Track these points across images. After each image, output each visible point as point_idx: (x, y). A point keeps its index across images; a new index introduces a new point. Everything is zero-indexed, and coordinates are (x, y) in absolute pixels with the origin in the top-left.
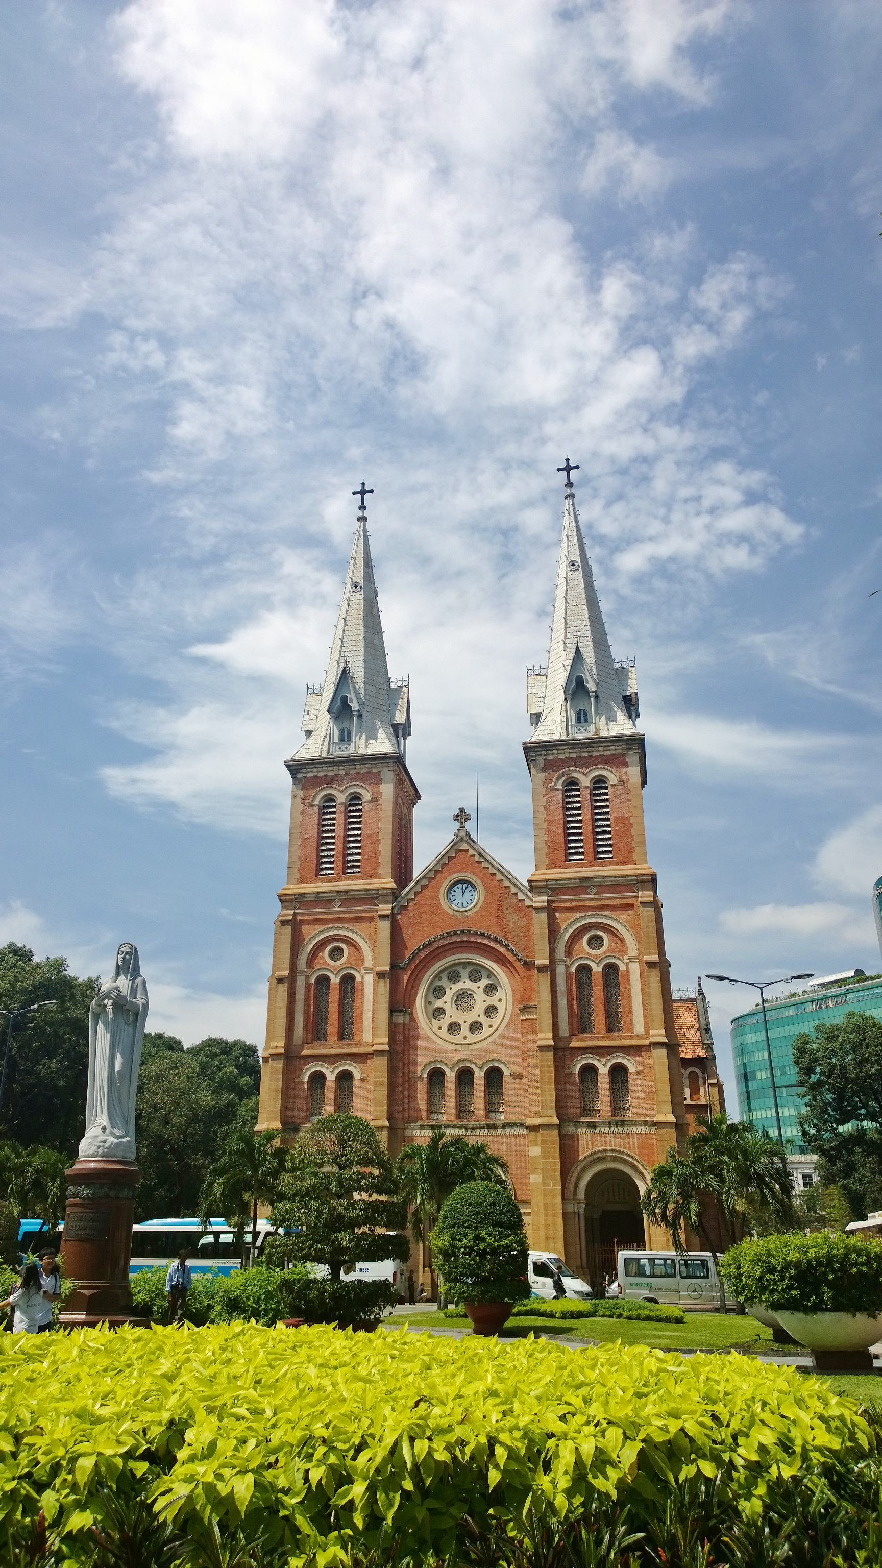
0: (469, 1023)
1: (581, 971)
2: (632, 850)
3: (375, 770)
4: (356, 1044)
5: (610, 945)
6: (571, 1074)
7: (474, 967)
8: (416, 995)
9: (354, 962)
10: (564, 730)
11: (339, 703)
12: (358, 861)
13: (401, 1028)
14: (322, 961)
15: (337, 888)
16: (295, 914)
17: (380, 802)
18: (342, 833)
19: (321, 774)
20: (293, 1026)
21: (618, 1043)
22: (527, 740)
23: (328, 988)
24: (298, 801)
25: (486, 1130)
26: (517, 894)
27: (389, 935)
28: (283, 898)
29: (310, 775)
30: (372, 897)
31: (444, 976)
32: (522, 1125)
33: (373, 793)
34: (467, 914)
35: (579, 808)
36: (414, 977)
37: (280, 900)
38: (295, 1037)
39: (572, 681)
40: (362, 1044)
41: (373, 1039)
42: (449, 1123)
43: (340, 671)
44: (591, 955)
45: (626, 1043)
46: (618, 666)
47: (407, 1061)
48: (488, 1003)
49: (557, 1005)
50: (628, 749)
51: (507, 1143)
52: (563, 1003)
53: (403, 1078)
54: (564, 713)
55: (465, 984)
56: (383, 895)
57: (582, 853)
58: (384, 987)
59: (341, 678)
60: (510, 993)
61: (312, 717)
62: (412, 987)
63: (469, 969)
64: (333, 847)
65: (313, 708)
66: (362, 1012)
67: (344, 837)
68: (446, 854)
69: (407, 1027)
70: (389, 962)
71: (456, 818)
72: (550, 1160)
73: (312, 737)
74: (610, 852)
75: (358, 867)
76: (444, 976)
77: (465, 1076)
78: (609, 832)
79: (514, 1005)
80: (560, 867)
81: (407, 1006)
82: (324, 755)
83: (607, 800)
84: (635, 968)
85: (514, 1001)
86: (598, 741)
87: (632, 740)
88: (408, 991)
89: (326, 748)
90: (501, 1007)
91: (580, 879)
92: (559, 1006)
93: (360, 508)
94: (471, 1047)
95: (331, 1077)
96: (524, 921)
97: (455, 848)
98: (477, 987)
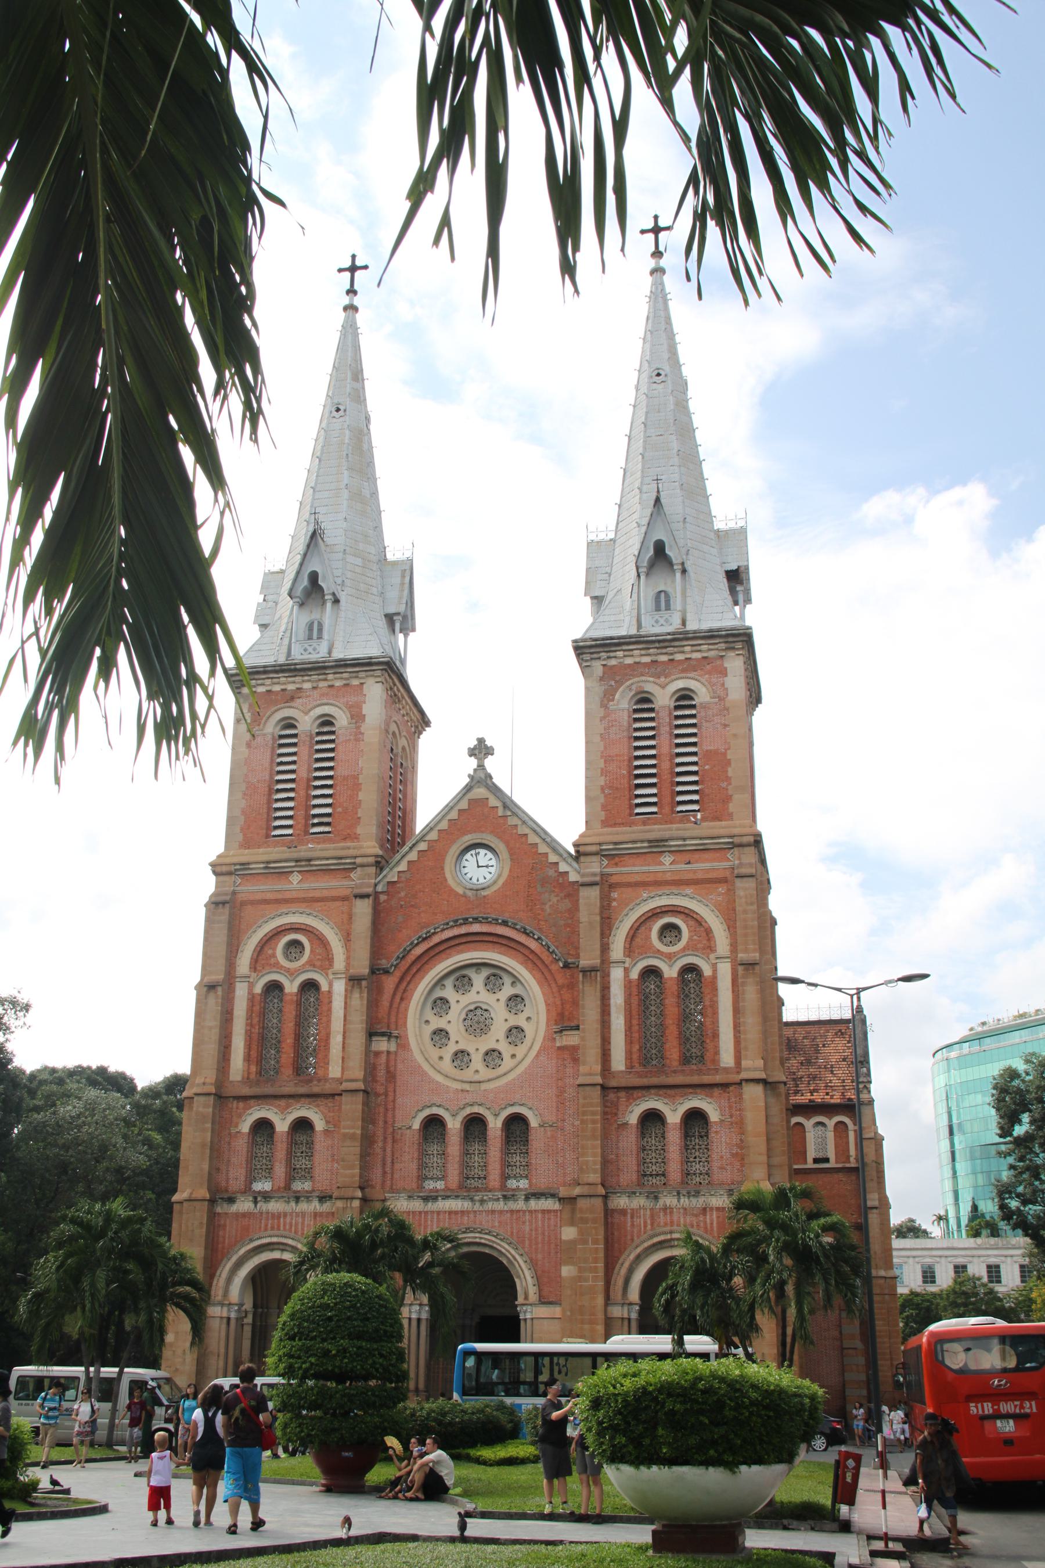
0: (483, 1049)
1: (649, 977)
2: (728, 799)
3: (355, 682)
5: (690, 939)
6: (626, 1124)
8: (407, 1010)
9: (318, 963)
10: (635, 622)
11: (305, 582)
12: (328, 815)
13: (384, 1057)
14: (272, 961)
15: (295, 855)
16: (234, 893)
17: (362, 730)
18: (305, 775)
19: (277, 688)
20: (230, 1054)
21: (695, 1079)
22: (578, 635)
23: (281, 1001)
25: (502, 1203)
26: (557, 863)
28: (218, 869)
29: (261, 689)
31: (449, 982)
32: (553, 1196)
34: (484, 893)
35: (653, 737)
36: (404, 984)
37: (215, 873)
38: (231, 1071)
39: (648, 548)
41: (343, 1073)
42: (449, 1194)
43: (310, 534)
44: (662, 953)
45: (707, 1079)
46: (719, 525)
47: (390, 1106)
48: (514, 1021)
49: (609, 1027)
50: (727, 649)
51: (530, 1222)
52: (618, 1022)
53: (385, 1129)
54: (635, 596)
55: (478, 993)
56: (362, 866)
58: (359, 1001)
59: (308, 546)
62: (402, 999)
63: (485, 972)
64: (292, 795)
67: (309, 780)
69: (392, 1057)
70: (367, 963)
71: (472, 752)
72: (590, 1245)
73: (269, 632)
75: (328, 824)
77: (475, 1125)
78: (695, 773)
79: (547, 1023)
80: (623, 824)
81: (393, 1026)
82: (282, 660)
83: (694, 725)
84: (725, 970)
88: (395, 1005)
89: (285, 649)
91: (650, 841)
92: (613, 1027)
94: (484, 1086)
95: (282, 1126)
96: (567, 904)
97: (470, 796)
98: (496, 1003)
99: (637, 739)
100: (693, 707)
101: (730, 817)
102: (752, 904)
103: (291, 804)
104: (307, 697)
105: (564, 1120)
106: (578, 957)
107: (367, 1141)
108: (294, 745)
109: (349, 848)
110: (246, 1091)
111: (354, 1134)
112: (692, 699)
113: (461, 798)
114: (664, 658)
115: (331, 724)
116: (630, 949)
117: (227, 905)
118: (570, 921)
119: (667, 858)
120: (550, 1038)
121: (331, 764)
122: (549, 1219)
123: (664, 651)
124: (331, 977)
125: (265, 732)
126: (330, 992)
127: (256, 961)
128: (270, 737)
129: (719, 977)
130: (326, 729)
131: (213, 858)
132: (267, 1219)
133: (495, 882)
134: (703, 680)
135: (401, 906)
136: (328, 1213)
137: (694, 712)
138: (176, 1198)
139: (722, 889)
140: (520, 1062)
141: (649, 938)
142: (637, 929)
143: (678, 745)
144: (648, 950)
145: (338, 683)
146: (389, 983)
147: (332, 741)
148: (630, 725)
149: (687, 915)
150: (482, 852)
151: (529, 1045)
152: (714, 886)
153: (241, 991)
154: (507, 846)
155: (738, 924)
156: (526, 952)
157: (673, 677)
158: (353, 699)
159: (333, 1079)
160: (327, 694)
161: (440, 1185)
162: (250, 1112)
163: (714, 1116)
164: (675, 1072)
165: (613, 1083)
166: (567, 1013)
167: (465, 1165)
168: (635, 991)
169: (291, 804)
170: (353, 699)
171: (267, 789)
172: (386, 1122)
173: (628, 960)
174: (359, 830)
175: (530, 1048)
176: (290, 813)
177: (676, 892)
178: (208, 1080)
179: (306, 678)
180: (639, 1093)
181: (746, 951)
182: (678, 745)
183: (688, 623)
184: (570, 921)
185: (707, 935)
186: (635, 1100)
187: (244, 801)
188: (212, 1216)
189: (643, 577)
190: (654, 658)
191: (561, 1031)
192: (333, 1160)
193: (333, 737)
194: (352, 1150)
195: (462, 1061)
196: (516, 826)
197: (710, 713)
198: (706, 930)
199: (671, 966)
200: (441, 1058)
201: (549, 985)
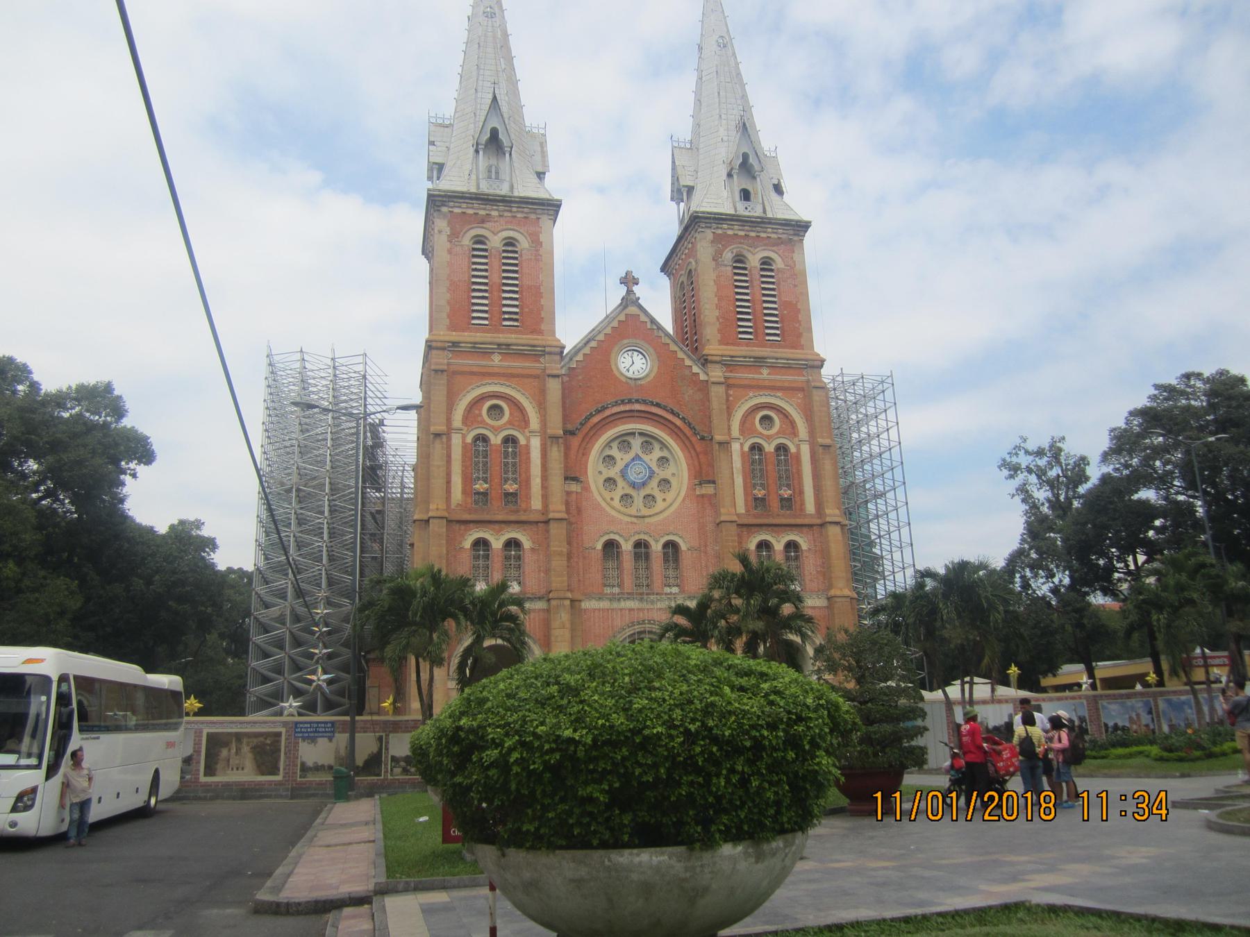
2: (799, 335)
3: (533, 216)
5: (781, 427)
7: (647, 439)
10: (731, 205)
14: (479, 419)
15: (497, 340)
16: (448, 364)
17: (541, 253)
19: (470, 211)
21: (792, 521)
27: (560, 397)
28: (434, 344)
29: (457, 210)
30: (536, 353)
31: (615, 445)
34: (642, 382)
36: (583, 445)
45: (799, 521)
50: (794, 235)
56: (550, 353)
58: (556, 453)
60: (684, 466)
61: (439, 149)
62: (583, 455)
64: (486, 295)
70: (560, 425)
75: (516, 320)
76: (615, 445)
82: (473, 190)
83: (773, 283)
84: (805, 450)
85: (689, 476)
86: (763, 222)
87: (800, 226)
89: (473, 183)
90: (674, 482)
91: (754, 358)
94: (647, 520)
95: (497, 543)
99: (737, 287)
100: (772, 270)
101: (802, 347)
104: (495, 222)
105: (706, 546)
107: (569, 556)
108: (485, 257)
111: (562, 551)
112: (770, 265)
113: (620, 312)
114: (753, 234)
116: (742, 431)
117: (445, 373)
118: (702, 408)
120: (692, 488)
123: (754, 229)
124: (528, 435)
126: (527, 447)
129: (802, 453)
130: (510, 249)
133: (647, 375)
134: (780, 252)
136: (540, 610)
137: (773, 274)
140: (671, 505)
141: (754, 424)
143: (764, 295)
145: (519, 215)
146: (575, 442)
147: (516, 258)
149: (778, 410)
150: (636, 353)
153: (456, 440)
154: (655, 350)
156: (673, 428)
160: (511, 222)
161: (616, 590)
163: (804, 546)
164: (778, 515)
166: (704, 472)
167: (637, 578)
172: (578, 544)
173: (741, 437)
174: (543, 327)
175: (678, 495)
176: (486, 308)
178: (440, 507)
179: (495, 207)
180: (756, 529)
182: (764, 295)
184: (702, 408)
186: (754, 533)
187: (449, 295)
189: (735, 177)
190: (747, 233)
191: (701, 484)
192: (540, 571)
193: (516, 255)
194: (558, 563)
195: (626, 502)
198: (791, 422)
199: (769, 444)
200: (612, 499)
201: (690, 452)
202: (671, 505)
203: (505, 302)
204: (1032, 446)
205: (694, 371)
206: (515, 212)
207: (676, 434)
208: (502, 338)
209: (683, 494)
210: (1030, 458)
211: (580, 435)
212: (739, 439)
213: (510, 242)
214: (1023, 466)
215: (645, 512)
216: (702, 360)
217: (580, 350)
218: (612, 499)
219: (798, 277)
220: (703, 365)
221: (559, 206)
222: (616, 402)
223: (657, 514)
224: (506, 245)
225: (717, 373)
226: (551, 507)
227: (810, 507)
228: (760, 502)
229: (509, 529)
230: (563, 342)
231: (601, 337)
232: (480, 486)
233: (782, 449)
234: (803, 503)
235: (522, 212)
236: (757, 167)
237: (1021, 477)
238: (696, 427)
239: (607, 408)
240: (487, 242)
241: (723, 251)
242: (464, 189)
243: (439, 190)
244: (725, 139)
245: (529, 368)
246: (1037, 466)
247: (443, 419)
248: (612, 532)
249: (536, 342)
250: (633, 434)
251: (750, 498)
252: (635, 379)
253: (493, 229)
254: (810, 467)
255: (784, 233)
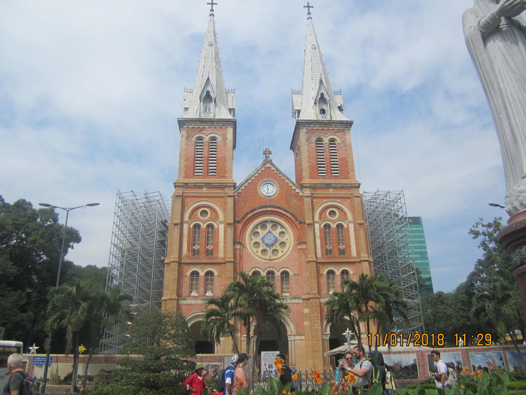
2: (348, 173)
3: (224, 127)
4: (215, 258)
5: (339, 216)
8: (245, 235)
9: (214, 218)
13: (239, 250)
15: (205, 182)
16: (183, 193)
17: (227, 142)
21: (345, 260)
24: (184, 138)
28: (177, 184)
30: (223, 186)
31: (259, 227)
33: (223, 138)
34: (272, 197)
35: (323, 152)
37: (175, 186)
39: (319, 95)
40: (218, 258)
44: (331, 220)
45: (348, 260)
52: (318, 241)
56: (229, 186)
57: (325, 173)
58: (230, 231)
64: (202, 162)
65: (188, 98)
66: (218, 243)
67: (208, 158)
68: (261, 169)
69: (241, 250)
74: (338, 173)
75: (215, 172)
76: (259, 227)
78: (337, 164)
79: (294, 241)
80: (315, 178)
82: (198, 117)
83: (336, 150)
84: (351, 226)
86: (330, 123)
89: (198, 114)
91: (326, 184)
93: (211, 11)
94: (273, 261)
95: (202, 273)
96: (299, 203)
97: (266, 166)
99: (318, 152)
100: (335, 144)
101: (350, 178)
102: (360, 205)
103: (202, 165)
106: (304, 219)
108: (202, 146)
109: (224, 180)
110: (189, 261)
111: (231, 276)
113: (262, 167)
115: (216, 140)
116: (320, 218)
118: (300, 208)
119: (331, 190)
121: (216, 153)
122: (299, 306)
125: (192, 140)
126: (218, 228)
127: (191, 217)
128: (194, 142)
129: (350, 228)
130: (213, 141)
131: (175, 181)
132: (198, 306)
133: (275, 194)
135: (243, 200)
137: (336, 146)
138: (163, 298)
139: (349, 200)
140: (285, 254)
141: (326, 215)
142: (322, 212)
143: (331, 155)
144: (326, 219)
145: (217, 127)
146: (240, 226)
147: (216, 146)
148: (316, 148)
149: (338, 208)
151: (288, 248)
152: (346, 199)
153: (186, 226)
155: (356, 211)
157: (329, 134)
158: (223, 132)
159: (220, 257)
160: (214, 130)
162: (190, 268)
164: (338, 258)
165: (318, 261)
168: (322, 232)
169: (202, 165)
170: (223, 132)
171: (193, 159)
173: (320, 221)
174: (227, 175)
176: (202, 168)
177: (335, 200)
178: (175, 257)
179: (207, 124)
181: (359, 220)
182: (331, 155)
183: (332, 118)
185: (345, 214)
186: (325, 267)
187: (185, 163)
188: (178, 305)
189: (317, 104)
193: (216, 144)
196: (281, 177)
197: (341, 146)
200: (257, 252)
202: (285, 254)
203: (210, 165)
204: (485, 223)
205: (297, 192)
206: (216, 126)
207: (288, 221)
208: (208, 180)
209: (291, 248)
210: (485, 228)
211: (242, 223)
212: (319, 222)
213: (213, 139)
214: (481, 232)
215: (274, 257)
216: (301, 186)
217: (243, 184)
218: (257, 252)
219: (347, 146)
220: (302, 189)
221: (236, 122)
222: (259, 207)
223: (278, 258)
224: (212, 140)
225: (307, 192)
226: (227, 256)
227: (354, 253)
228: (328, 252)
229: (208, 266)
230: (235, 181)
231: (253, 178)
232: (196, 247)
233: (340, 226)
234: (350, 252)
235: (219, 125)
236: (328, 98)
237: (481, 238)
238: (297, 217)
239: (255, 210)
240: (203, 139)
241: (311, 136)
242: (194, 117)
243: (182, 118)
244: (314, 88)
245: (219, 193)
246: (488, 232)
247: (179, 217)
248: (256, 267)
249: (223, 182)
250: (267, 221)
251: (324, 250)
252: (269, 196)
253: (205, 134)
254: (354, 234)
255: (340, 127)
